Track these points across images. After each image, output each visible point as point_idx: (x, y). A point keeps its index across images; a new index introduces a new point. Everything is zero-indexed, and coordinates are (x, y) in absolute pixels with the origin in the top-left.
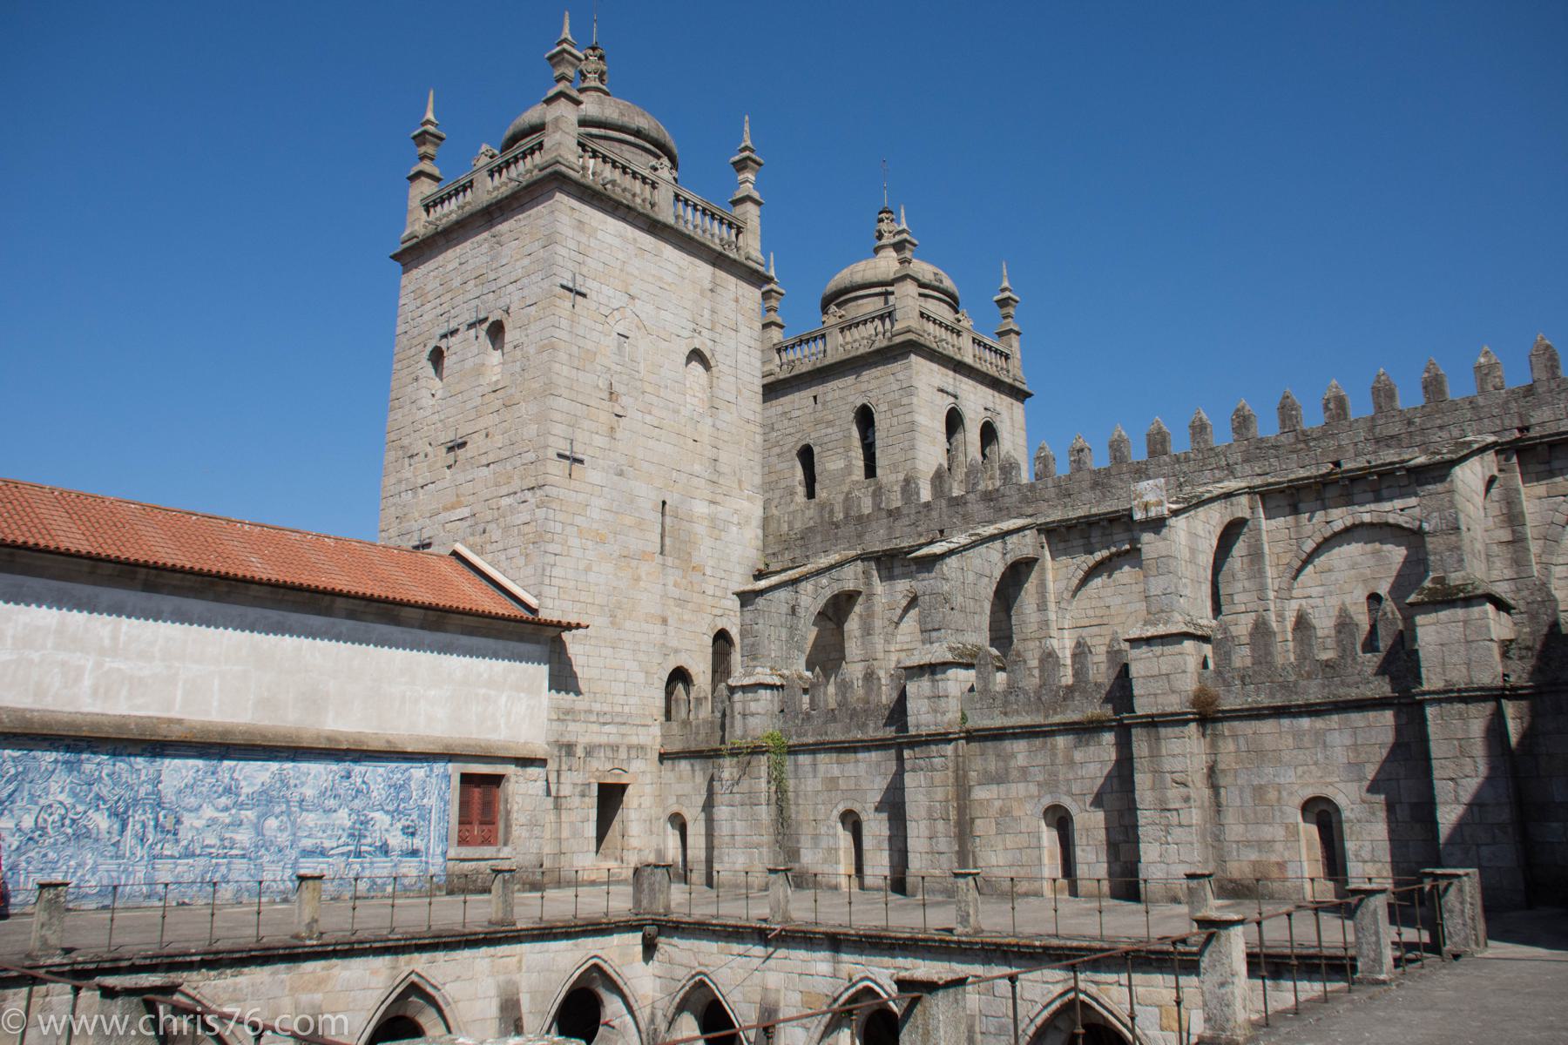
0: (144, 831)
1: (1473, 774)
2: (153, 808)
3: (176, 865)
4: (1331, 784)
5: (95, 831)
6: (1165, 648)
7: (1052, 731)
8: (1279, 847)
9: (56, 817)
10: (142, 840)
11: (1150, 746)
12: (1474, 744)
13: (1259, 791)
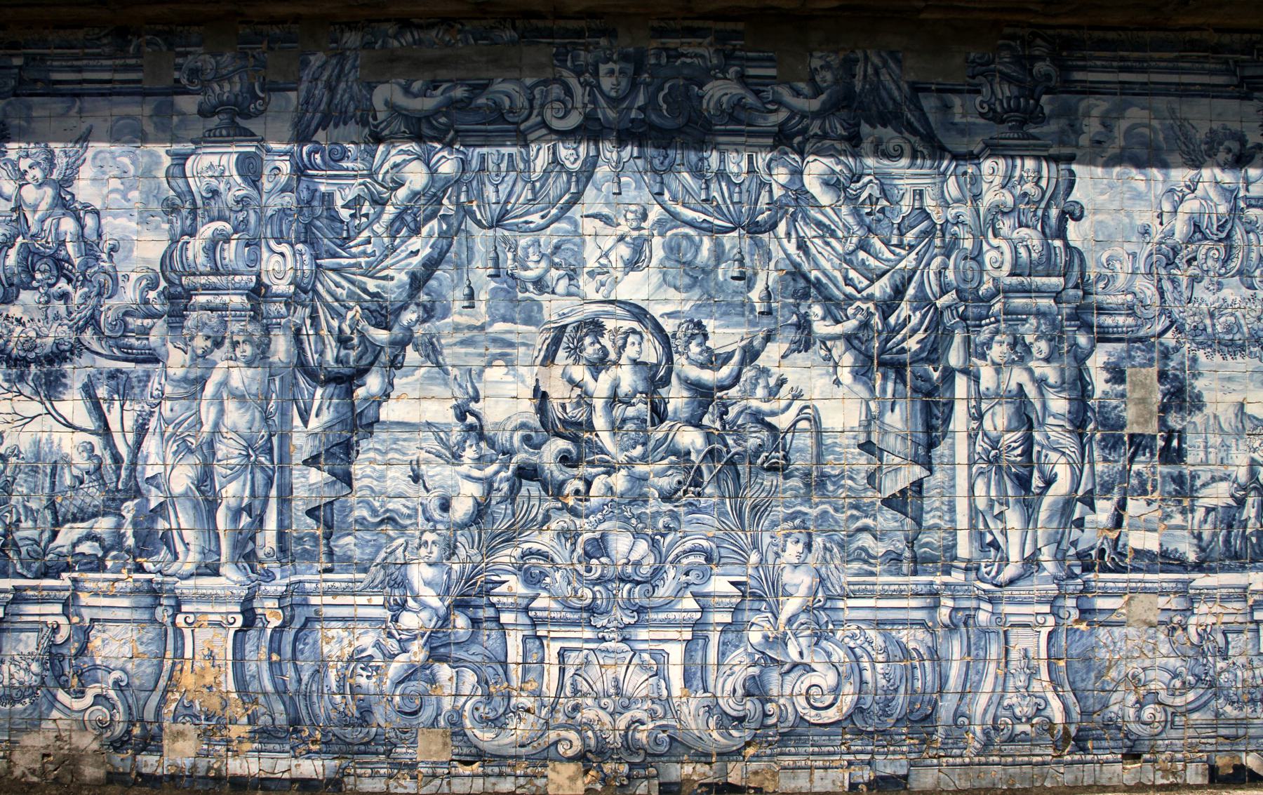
0: (1028, 441)
2: (1055, 337)
3: (1191, 598)
5: (804, 441)
9: (627, 378)
10: (1023, 482)
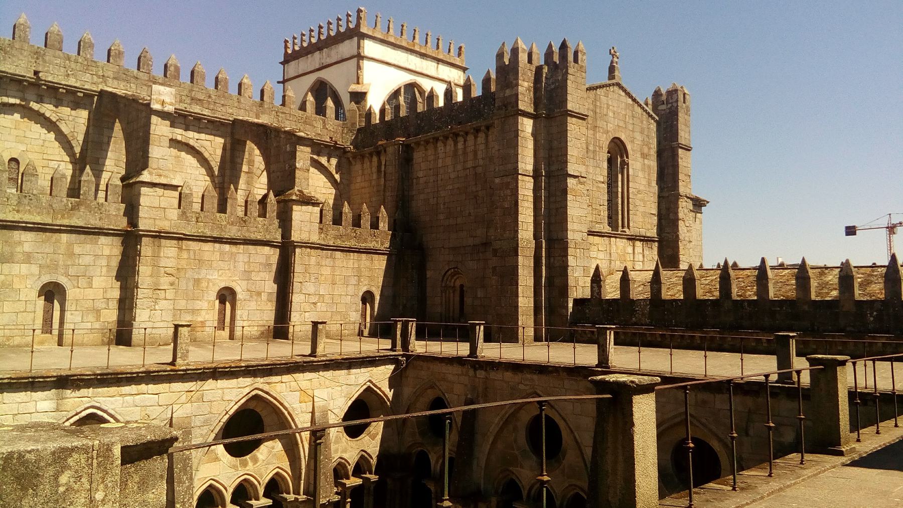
1: (308, 281)
4: (235, 281)
6: (166, 191)
7: (60, 230)
8: (203, 313)
11: (154, 251)
12: (311, 267)
13: (197, 281)
